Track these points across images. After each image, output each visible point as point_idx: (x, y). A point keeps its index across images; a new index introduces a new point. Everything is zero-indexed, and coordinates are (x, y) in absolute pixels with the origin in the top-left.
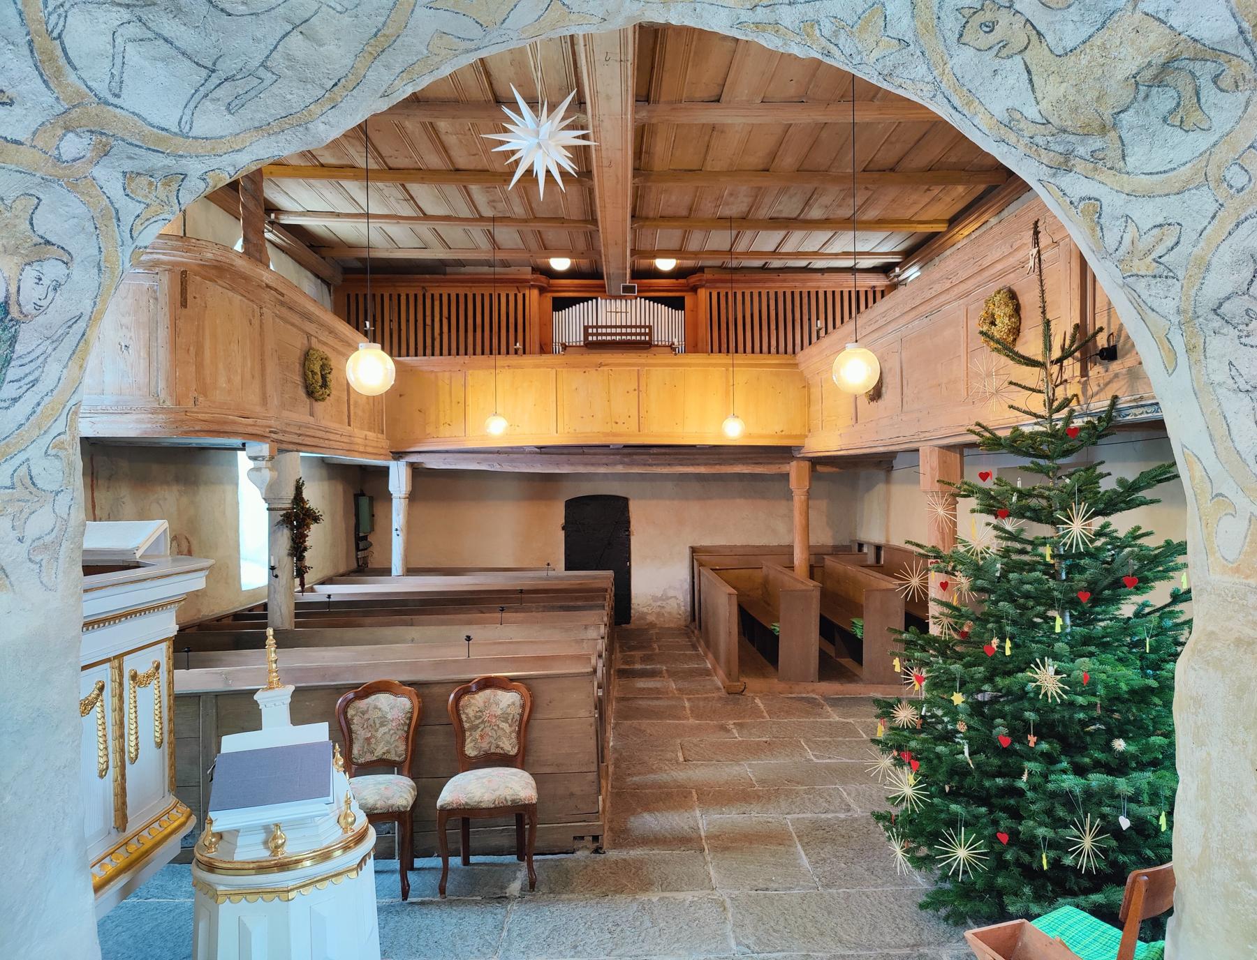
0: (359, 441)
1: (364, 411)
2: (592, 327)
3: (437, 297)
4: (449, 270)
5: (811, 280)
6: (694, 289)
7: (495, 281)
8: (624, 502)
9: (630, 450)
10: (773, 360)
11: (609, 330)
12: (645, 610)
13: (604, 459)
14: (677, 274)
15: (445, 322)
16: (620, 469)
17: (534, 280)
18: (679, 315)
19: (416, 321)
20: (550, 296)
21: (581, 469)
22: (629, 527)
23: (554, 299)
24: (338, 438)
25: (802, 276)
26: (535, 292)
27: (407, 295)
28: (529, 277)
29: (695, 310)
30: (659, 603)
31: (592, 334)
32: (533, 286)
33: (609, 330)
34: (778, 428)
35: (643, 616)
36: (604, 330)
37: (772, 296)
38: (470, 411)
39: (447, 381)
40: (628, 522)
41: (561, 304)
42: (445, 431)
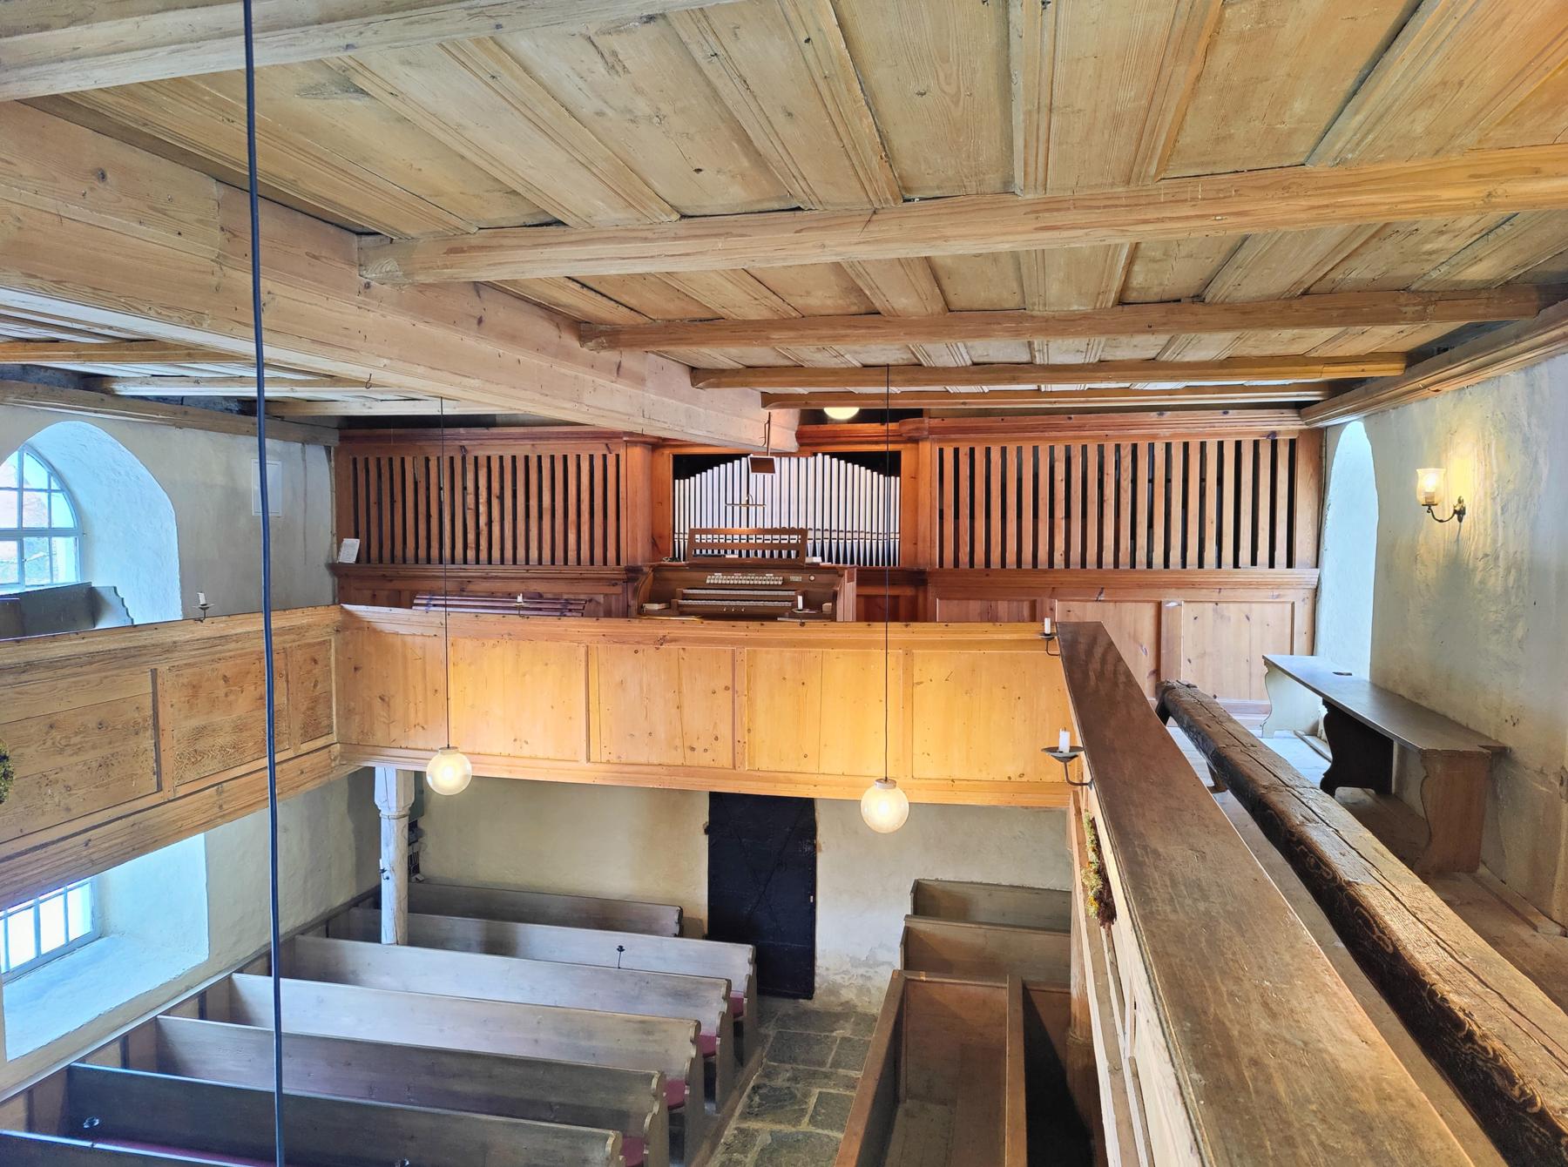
2: (702, 531)
3: (483, 462)
12: (838, 979)
15: (495, 503)
22: (814, 836)
23: (677, 458)
30: (862, 971)
31: (702, 546)
34: (1012, 770)
35: (833, 990)
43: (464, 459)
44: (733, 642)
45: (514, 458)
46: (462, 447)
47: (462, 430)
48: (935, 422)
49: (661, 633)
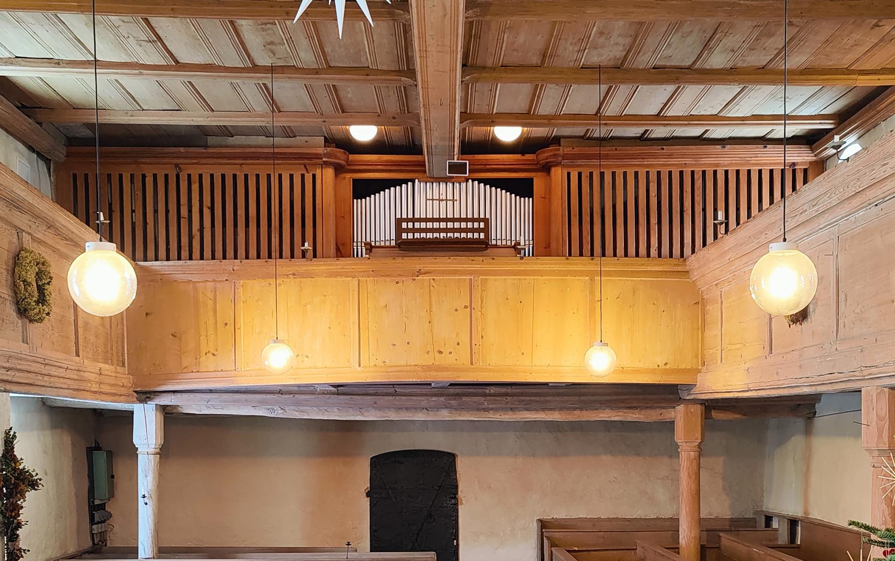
0: (92, 376)
1: (97, 336)
2: (407, 220)
4: (211, 140)
5: (708, 155)
6: (546, 169)
7: (275, 156)
8: (451, 458)
9: (458, 390)
10: (656, 266)
11: (430, 225)
13: (424, 401)
14: (524, 146)
16: (445, 415)
17: (325, 155)
18: (527, 202)
19: (167, 212)
20: (349, 176)
21: (393, 416)
24: (61, 373)
25: (693, 149)
26: (329, 172)
27: (155, 176)
28: (321, 151)
29: (548, 197)
31: (407, 230)
32: (327, 164)
33: (430, 225)
34: (660, 360)
36: (423, 225)
37: (653, 178)
38: (241, 333)
39: (210, 295)
40: (454, 488)
41: (365, 189)
42: (209, 363)
43: (178, 176)
44: (471, 273)
45: (223, 176)
46: (177, 165)
47: (182, 149)
48: (568, 150)
49: (418, 267)
